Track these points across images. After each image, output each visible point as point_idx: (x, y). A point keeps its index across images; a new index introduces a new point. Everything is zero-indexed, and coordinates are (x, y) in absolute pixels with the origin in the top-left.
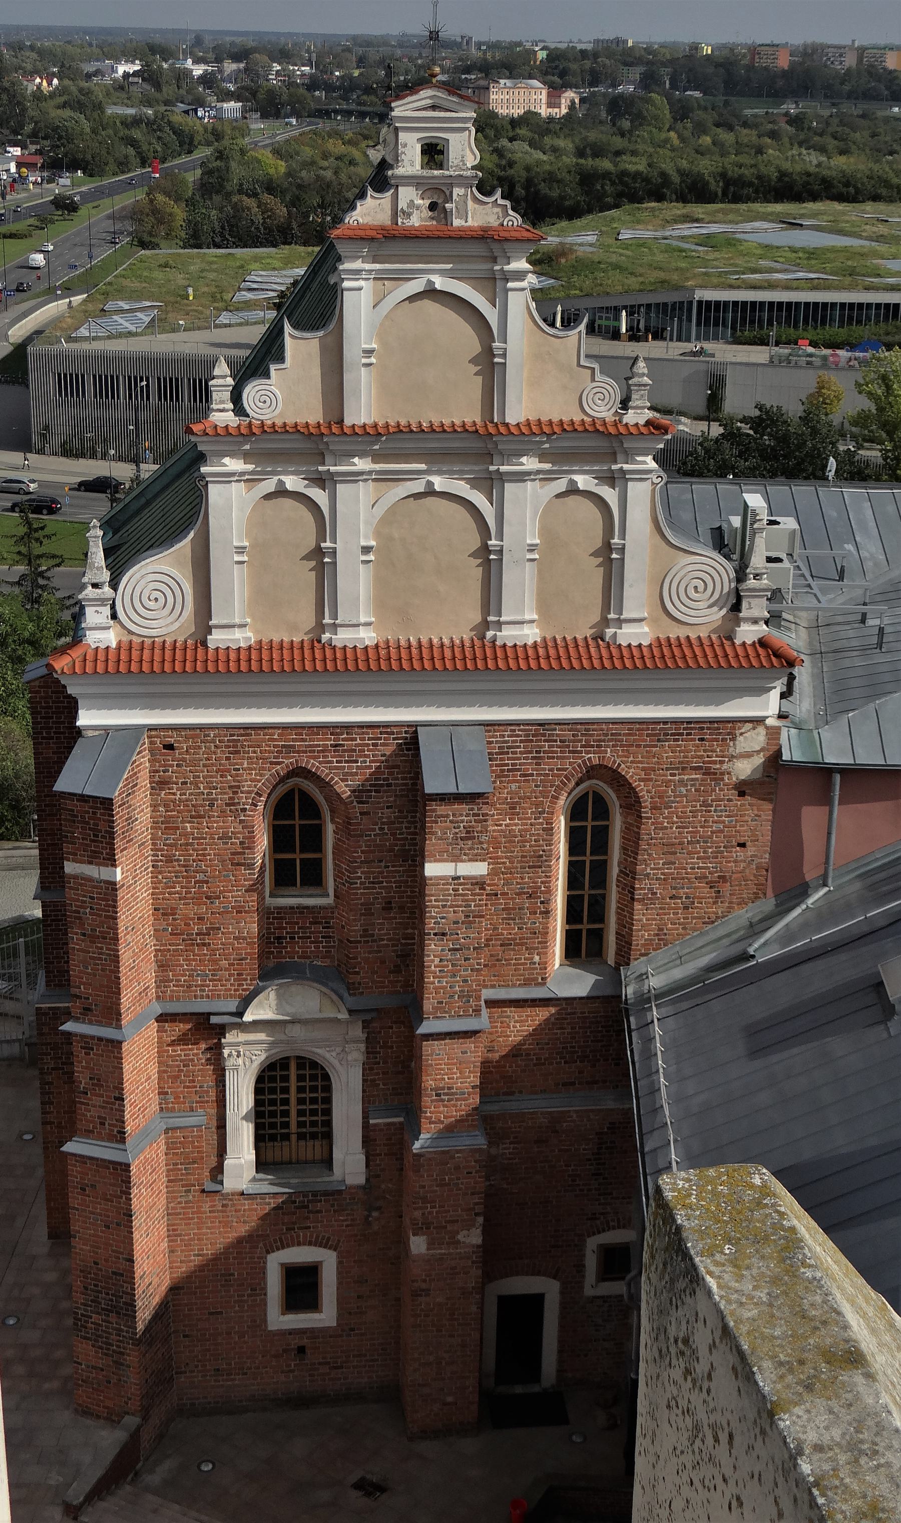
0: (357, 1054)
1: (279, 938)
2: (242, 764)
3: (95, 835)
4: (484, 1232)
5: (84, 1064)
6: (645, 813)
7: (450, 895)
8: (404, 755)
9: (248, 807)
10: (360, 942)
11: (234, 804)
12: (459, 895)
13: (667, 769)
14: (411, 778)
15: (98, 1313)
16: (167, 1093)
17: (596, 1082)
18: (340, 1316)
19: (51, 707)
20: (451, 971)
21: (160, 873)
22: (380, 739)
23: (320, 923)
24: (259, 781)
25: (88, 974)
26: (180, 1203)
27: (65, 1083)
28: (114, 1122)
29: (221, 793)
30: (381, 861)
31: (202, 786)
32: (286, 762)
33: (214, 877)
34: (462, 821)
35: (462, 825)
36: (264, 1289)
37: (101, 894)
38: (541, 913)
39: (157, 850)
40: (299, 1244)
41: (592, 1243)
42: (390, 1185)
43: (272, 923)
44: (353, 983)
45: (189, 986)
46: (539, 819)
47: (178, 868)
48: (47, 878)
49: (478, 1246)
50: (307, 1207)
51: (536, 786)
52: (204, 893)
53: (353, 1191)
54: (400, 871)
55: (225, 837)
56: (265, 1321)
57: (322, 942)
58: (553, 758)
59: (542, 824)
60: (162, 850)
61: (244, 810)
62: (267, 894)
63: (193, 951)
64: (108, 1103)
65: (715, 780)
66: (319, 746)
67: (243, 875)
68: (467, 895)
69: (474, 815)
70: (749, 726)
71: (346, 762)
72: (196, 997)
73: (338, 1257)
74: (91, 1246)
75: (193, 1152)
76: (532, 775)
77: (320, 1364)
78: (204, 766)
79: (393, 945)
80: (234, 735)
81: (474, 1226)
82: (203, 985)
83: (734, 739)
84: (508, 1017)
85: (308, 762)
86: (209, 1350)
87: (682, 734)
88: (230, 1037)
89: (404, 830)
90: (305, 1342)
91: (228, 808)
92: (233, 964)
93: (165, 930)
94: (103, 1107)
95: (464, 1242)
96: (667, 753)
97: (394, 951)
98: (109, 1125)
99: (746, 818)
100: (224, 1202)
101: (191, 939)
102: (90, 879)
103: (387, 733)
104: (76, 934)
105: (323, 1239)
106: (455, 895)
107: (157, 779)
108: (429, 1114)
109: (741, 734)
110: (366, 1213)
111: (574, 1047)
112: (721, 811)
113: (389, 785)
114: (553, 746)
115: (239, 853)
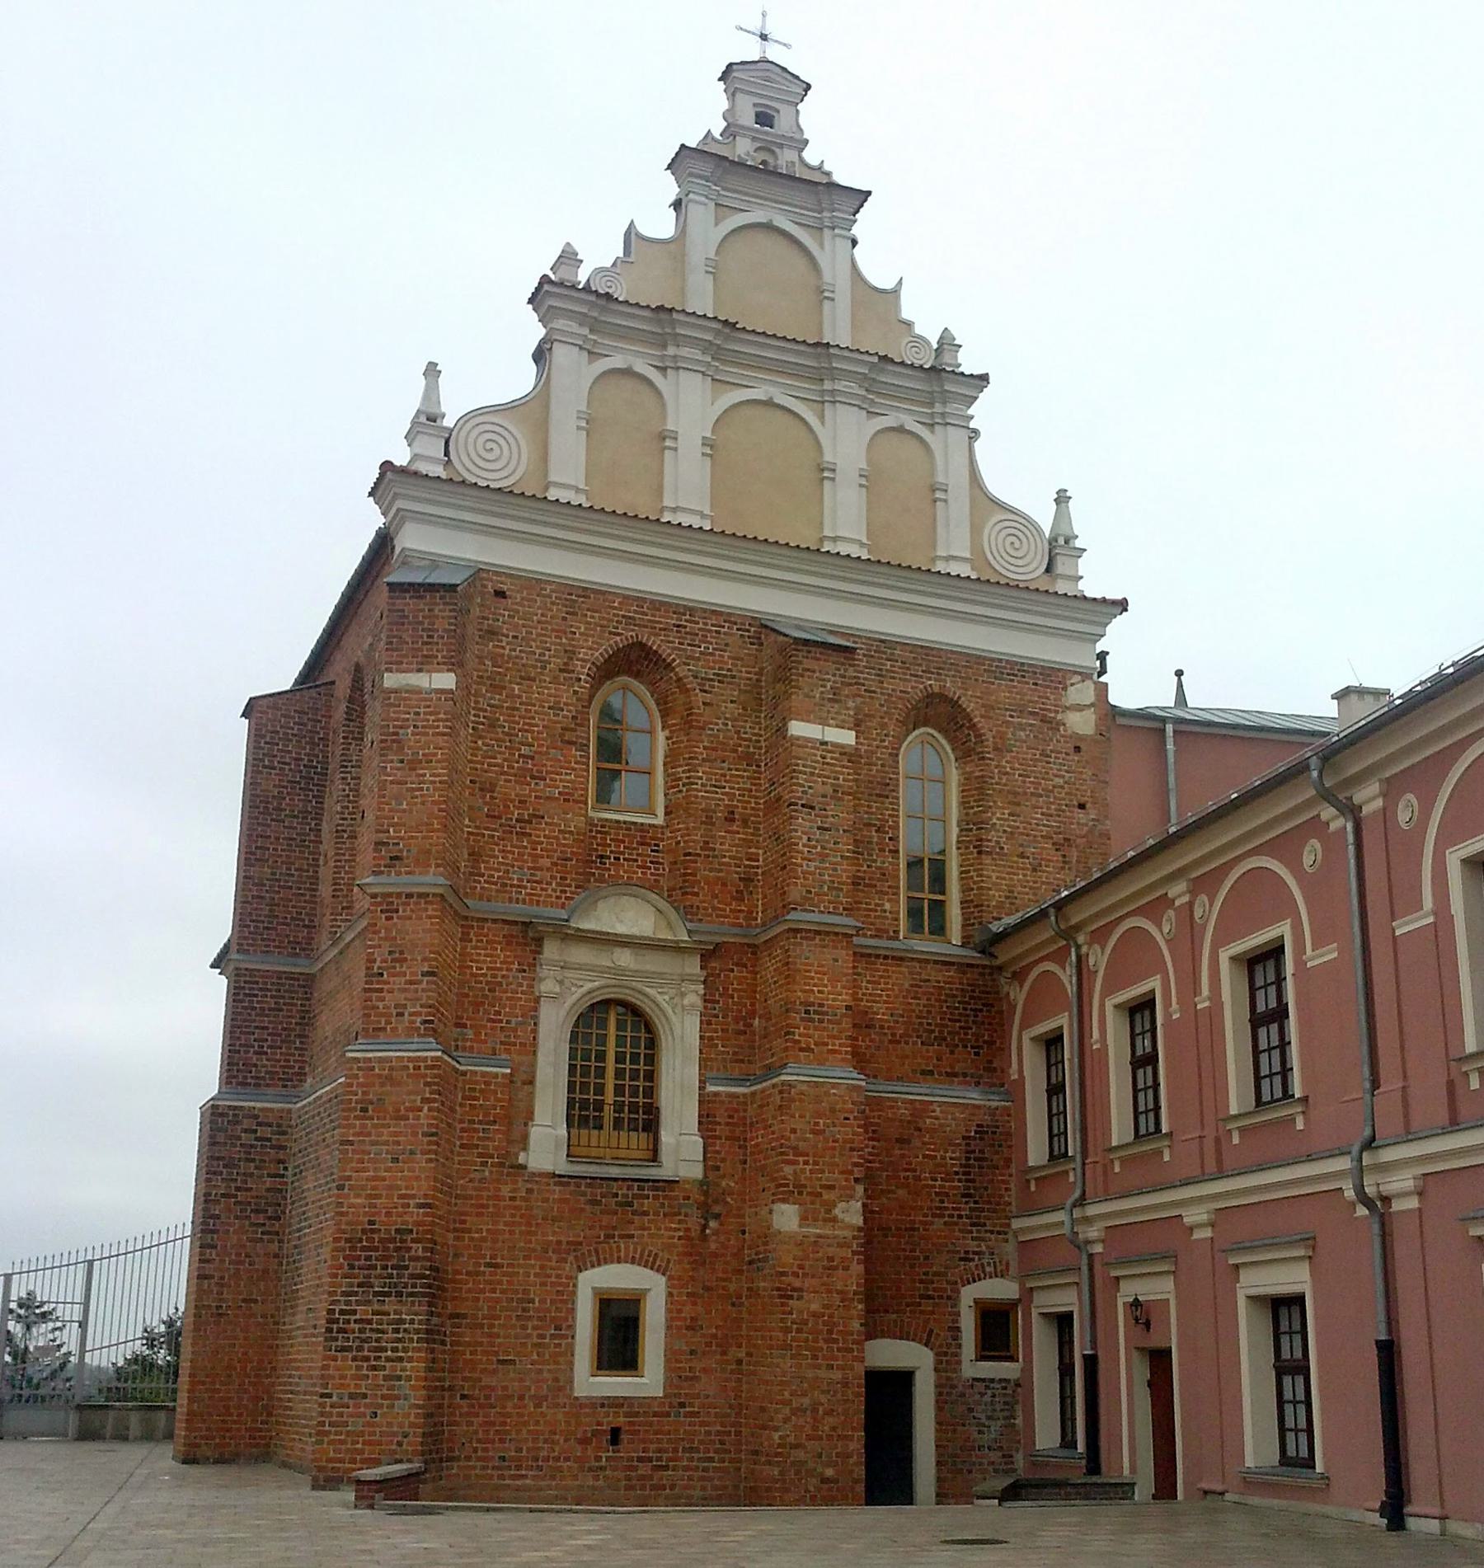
0: (694, 997)
1: (602, 857)
3: (429, 637)
5: (382, 934)
10: (699, 855)
12: (828, 764)
13: (1007, 710)
16: (464, 1026)
17: (955, 1075)
18: (668, 1383)
20: (819, 854)
21: (480, 737)
23: (649, 845)
25: (404, 811)
31: (533, 644)
33: (540, 753)
36: (571, 1327)
37: (429, 707)
38: (890, 851)
41: (969, 1294)
46: (884, 741)
47: (501, 735)
49: (860, 1229)
50: (630, 1204)
54: (743, 777)
55: (556, 708)
58: (894, 678)
59: (886, 747)
60: (486, 711)
64: (411, 983)
65: (1052, 729)
66: (661, 623)
70: (1077, 678)
71: (689, 645)
76: (874, 692)
77: (640, 1459)
81: (852, 1197)
82: (519, 886)
83: (1065, 689)
86: (493, 1424)
87: (1016, 676)
92: (556, 864)
94: (405, 990)
95: (843, 1221)
97: (737, 873)
98: (411, 1015)
99: (1084, 776)
100: (530, 1186)
102: (417, 691)
104: (392, 761)
105: (649, 1256)
107: (485, 627)
108: (797, 1037)
109: (1072, 685)
110: (703, 1222)
113: (733, 677)
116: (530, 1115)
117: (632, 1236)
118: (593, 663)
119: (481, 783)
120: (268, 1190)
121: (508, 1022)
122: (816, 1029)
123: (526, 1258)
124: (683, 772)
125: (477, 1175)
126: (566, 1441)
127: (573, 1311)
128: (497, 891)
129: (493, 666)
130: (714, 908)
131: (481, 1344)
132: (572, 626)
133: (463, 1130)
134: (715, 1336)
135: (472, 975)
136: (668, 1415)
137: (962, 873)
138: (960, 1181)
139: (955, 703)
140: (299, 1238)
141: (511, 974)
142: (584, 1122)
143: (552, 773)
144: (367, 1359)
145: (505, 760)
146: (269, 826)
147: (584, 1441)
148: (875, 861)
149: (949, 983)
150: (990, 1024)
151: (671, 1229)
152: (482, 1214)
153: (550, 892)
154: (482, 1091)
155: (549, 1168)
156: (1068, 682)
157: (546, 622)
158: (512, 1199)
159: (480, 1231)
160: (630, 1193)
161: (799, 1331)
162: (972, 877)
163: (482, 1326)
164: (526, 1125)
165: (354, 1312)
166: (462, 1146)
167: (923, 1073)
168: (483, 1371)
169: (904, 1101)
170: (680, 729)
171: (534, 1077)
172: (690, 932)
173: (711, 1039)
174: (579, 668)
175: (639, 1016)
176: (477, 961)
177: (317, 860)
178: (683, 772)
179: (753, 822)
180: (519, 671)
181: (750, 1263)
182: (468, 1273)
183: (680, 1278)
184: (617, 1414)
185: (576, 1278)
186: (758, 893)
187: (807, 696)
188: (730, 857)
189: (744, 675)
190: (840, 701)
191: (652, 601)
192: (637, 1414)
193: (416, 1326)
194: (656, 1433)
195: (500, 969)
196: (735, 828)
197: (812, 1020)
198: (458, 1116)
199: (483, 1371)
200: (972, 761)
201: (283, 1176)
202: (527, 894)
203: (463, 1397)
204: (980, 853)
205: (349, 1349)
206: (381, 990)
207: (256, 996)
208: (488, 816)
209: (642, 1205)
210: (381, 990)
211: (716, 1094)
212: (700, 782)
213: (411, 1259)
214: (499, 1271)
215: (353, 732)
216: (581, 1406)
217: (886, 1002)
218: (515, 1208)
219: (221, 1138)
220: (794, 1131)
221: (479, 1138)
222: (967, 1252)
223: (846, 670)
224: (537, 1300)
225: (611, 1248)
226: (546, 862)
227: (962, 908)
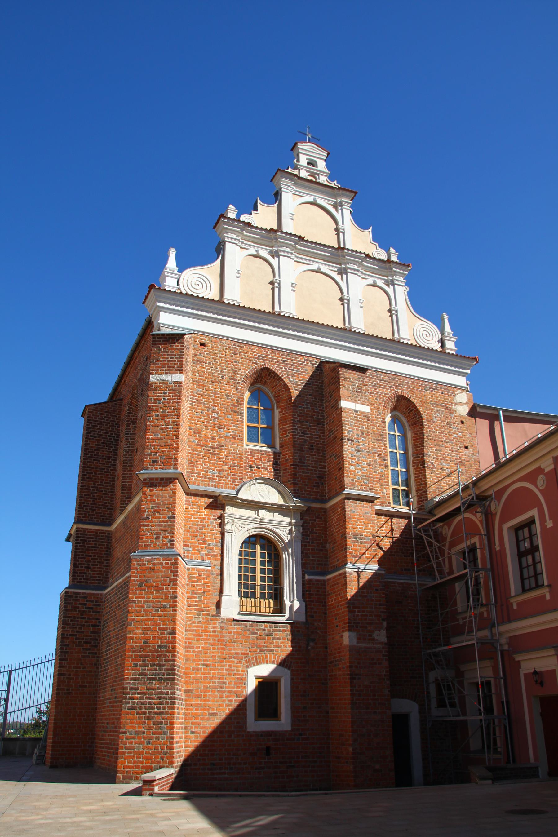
1: (251, 467)
2: (239, 360)
3: (171, 358)
5: (149, 498)
6: (425, 422)
7: (353, 420)
9: (241, 382)
10: (298, 465)
11: (234, 379)
12: (358, 421)
13: (431, 404)
14: (320, 383)
15: (144, 683)
19: (97, 421)
21: (194, 408)
22: (304, 362)
24: (247, 370)
26: (194, 622)
28: (167, 535)
29: (228, 372)
30: (307, 422)
31: (218, 367)
32: (260, 364)
33: (222, 416)
38: (385, 466)
39: (193, 395)
40: (267, 662)
41: (432, 676)
42: (320, 624)
45: (206, 478)
46: (379, 415)
47: (203, 408)
48: (82, 514)
49: (386, 644)
50: (271, 634)
51: (376, 399)
52: (216, 424)
53: (298, 625)
54: (316, 429)
56: (246, 723)
58: (382, 388)
59: (380, 418)
60: (196, 396)
61: (239, 383)
66: (276, 359)
68: (361, 421)
70: (459, 391)
73: (291, 675)
74: (144, 629)
76: (373, 393)
78: (220, 357)
79: (315, 470)
80: (235, 345)
82: (213, 479)
83: (454, 395)
85: (270, 366)
88: (229, 510)
89: (318, 408)
91: (231, 381)
92: (230, 468)
94: (159, 526)
97: (316, 474)
98: (163, 537)
100: (222, 625)
101: (208, 450)
103: (307, 360)
107: (196, 359)
109: (457, 394)
111: (407, 547)
114: (381, 382)
115: (236, 406)
117: (273, 650)
118: (246, 376)
119: (194, 429)
120: (92, 633)
123: (222, 661)
124: (289, 427)
125: (196, 620)
128: (202, 481)
129: (199, 376)
130: (306, 491)
131: (201, 705)
132: (235, 359)
135: (191, 521)
137: (416, 477)
139: (408, 400)
140: (107, 655)
141: (210, 521)
143: (227, 425)
144: (144, 713)
145: (205, 419)
146: (93, 463)
148: (378, 470)
152: (199, 639)
154: (197, 578)
156: (456, 393)
157: (224, 357)
158: (214, 632)
159: (198, 648)
162: (421, 479)
163: (200, 696)
165: (137, 688)
167: (405, 570)
168: (202, 719)
169: (398, 583)
170: (286, 408)
173: (306, 553)
174: (239, 378)
175: (271, 543)
177: (114, 478)
178: (289, 427)
179: (322, 451)
180: (211, 378)
182: (193, 669)
187: (347, 390)
188: (312, 467)
193: (169, 695)
195: (204, 519)
196: (313, 453)
197: (357, 542)
199: (202, 719)
200: (418, 426)
201: (98, 626)
202: (216, 482)
205: (135, 708)
206: (148, 526)
208: (197, 445)
209: (277, 635)
210: (148, 526)
211: (310, 580)
212: (296, 431)
213: (166, 661)
215: (131, 419)
219: (69, 607)
221: (197, 601)
224: (227, 682)
225: (263, 656)
226: (225, 467)
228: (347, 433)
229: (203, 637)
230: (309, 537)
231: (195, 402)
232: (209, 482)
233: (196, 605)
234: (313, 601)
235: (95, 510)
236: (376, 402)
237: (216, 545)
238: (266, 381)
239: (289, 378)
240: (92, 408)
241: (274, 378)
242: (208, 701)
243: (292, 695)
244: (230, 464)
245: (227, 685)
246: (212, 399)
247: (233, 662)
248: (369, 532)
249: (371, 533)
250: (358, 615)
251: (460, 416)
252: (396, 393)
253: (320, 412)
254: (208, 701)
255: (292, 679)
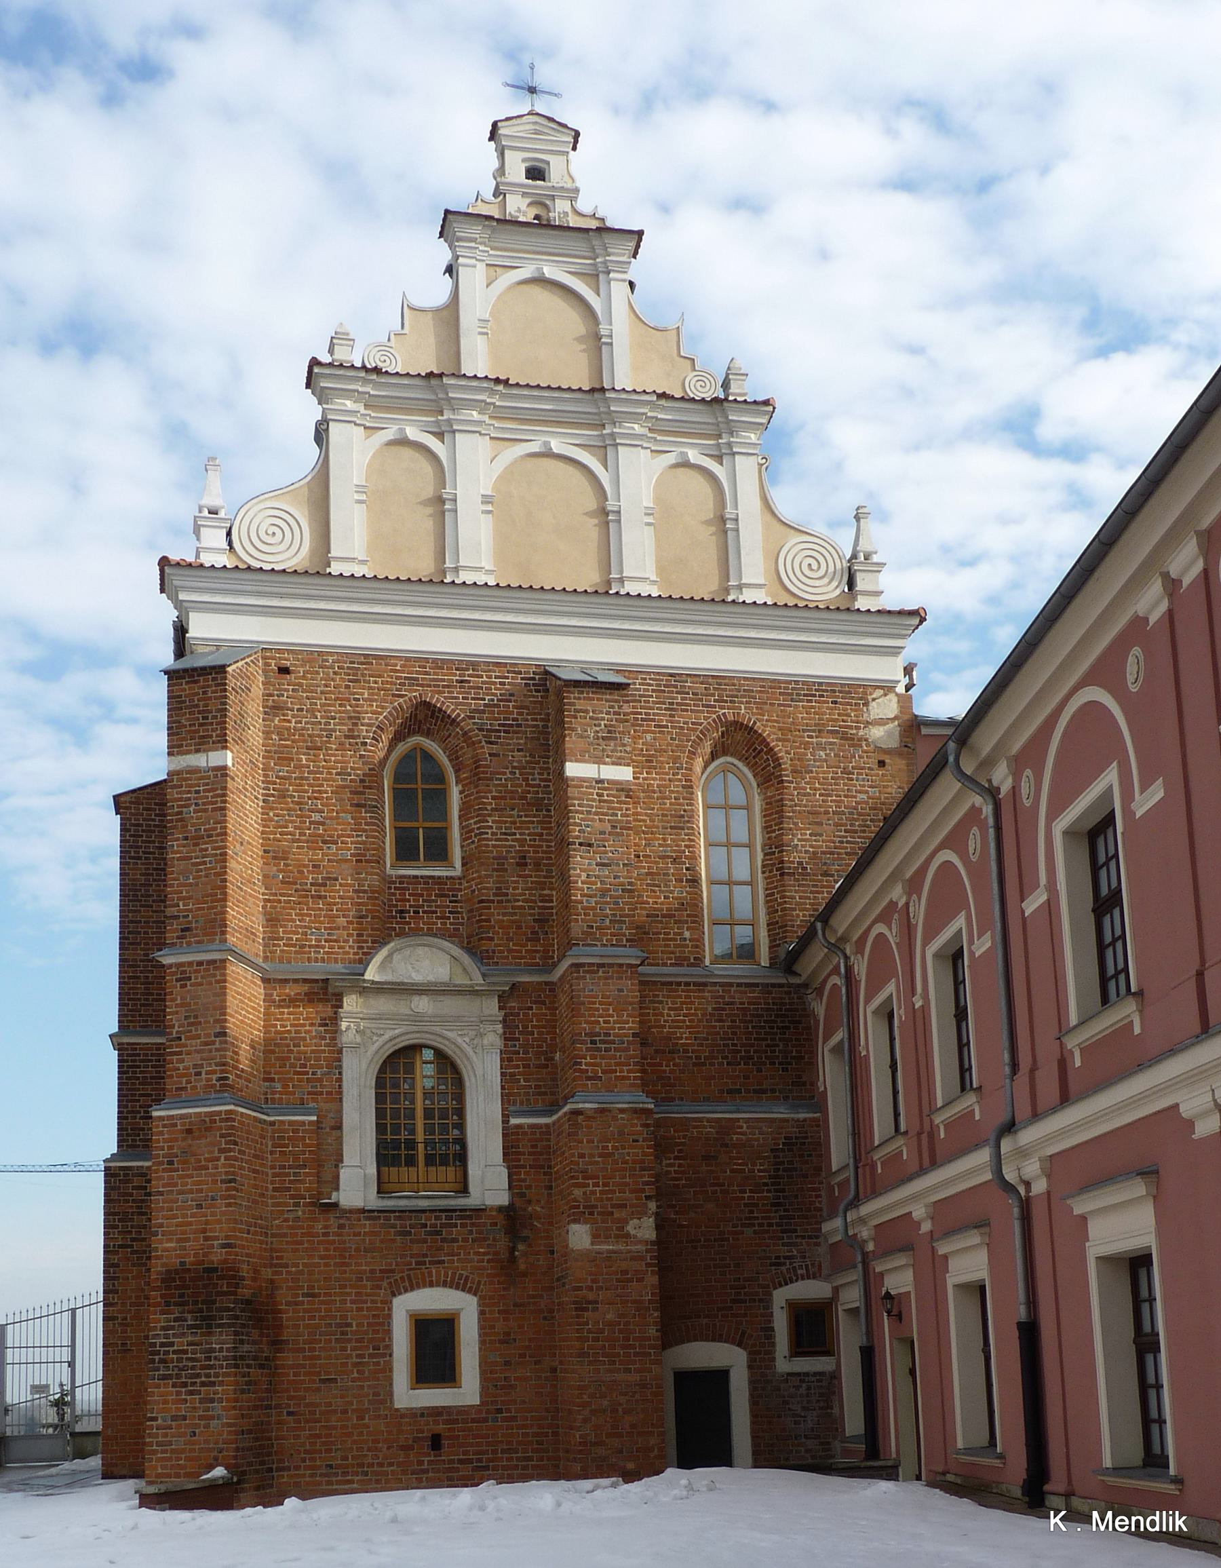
0: (493, 1037)
1: (401, 912)
4: (658, 1227)
6: (787, 776)
7: (594, 800)
8: (534, 696)
10: (493, 901)
11: (353, 737)
12: (605, 801)
13: (804, 731)
14: (542, 720)
16: (272, 1080)
21: (272, 809)
24: (380, 714)
25: (191, 885)
26: (286, 1220)
27: (134, 1265)
30: (513, 809)
32: (409, 695)
33: (331, 818)
34: (603, 719)
35: (602, 723)
40: (431, 1285)
43: (394, 894)
44: (487, 951)
46: (678, 774)
48: (126, 1016)
49: (653, 1243)
50: (438, 1233)
51: (671, 739)
52: (320, 835)
54: (533, 822)
56: (391, 1394)
57: (449, 918)
58: (687, 710)
59: (680, 780)
62: (388, 865)
63: (307, 904)
64: (206, 1044)
65: (853, 746)
67: (365, 818)
68: (613, 802)
69: (615, 713)
70: (879, 692)
71: (473, 699)
72: (309, 960)
73: (479, 1305)
75: (304, 1152)
76: (667, 727)
77: (461, 1461)
79: (530, 908)
81: (645, 1213)
82: (317, 946)
83: (866, 704)
84: (661, 1002)
85: (432, 697)
86: (318, 1436)
87: (815, 696)
89: (537, 776)
90: (441, 1428)
93: (275, 877)
95: (635, 1236)
96: (800, 713)
97: (531, 915)
100: (341, 1221)
105: (460, 1279)
106: (600, 801)
108: (584, 1067)
109: (874, 700)
110: (511, 1245)
111: (735, 1045)
112: (863, 780)
113: (519, 726)
114: (686, 699)
116: (340, 1159)
117: (443, 1262)
119: (274, 852)
121: (313, 1074)
122: (603, 1058)
124: (475, 823)
125: (291, 1216)
126: (388, 1448)
127: (389, 1332)
128: (296, 952)
130: (510, 951)
131: (304, 1366)
133: (275, 1175)
134: (528, 1348)
136: (485, 1420)
138: (769, 1191)
139: (750, 730)
142: (395, 1162)
143: (343, 836)
145: (296, 828)
147: (404, 1448)
149: (754, 1004)
150: (797, 1040)
151: (478, 1253)
153: (347, 949)
154: (289, 1138)
155: (358, 1203)
158: (325, 1234)
160: (439, 1222)
161: (596, 1339)
164: (337, 1166)
166: (275, 1189)
167: (730, 1092)
169: (709, 1120)
170: (470, 783)
171: (341, 1123)
172: (484, 975)
173: (512, 1075)
176: (282, 1020)
178: (475, 823)
179: (545, 865)
181: (558, 1280)
183: (491, 1298)
184: (436, 1422)
185: (391, 1302)
186: (553, 933)
187: (582, 737)
189: (530, 723)
190: (616, 739)
191: (435, 661)
192: (456, 1421)
194: (475, 1437)
195: (304, 1025)
197: (599, 1050)
198: (269, 1163)
199: (306, 1390)
200: (772, 785)
203: (289, 1414)
204: (782, 874)
206: (180, 1053)
207: (139, 1067)
208: (282, 882)
210: (180, 1053)
212: (490, 831)
214: (317, 1299)
216: (403, 1416)
217: (688, 1027)
218: (329, 1242)
219: (114, 1196)
220: (582, 1156)
222: (778, 1257)
223: (620, 707)
225: (423, 1274)
227: (769, 931)
228: (579, 831)
229: (306, 1245)
230: (517, 1043)
231: (273, 795)
232: (310, 953)
233: (289, 1189)
234: (523, 1167)
235: (151, 1005)
236: (671, 745)
237: (329, 1073)
238: (429, 729)
239: (474, 718)
240: (128, 798)
241: (442, 721)
242: (319, 1357)
243: (482, 1342)
244: (351, 913)
245: (354, 1328)
246: (309, 785)
247: (365, 1287)
248: (624, 1028)
249: (630, 1029)
250: (593, 1193)
251: (879, 749)
252: (720, 720)
253: (542, 784)
254: (319, 1357)
255: (482, 1313)
